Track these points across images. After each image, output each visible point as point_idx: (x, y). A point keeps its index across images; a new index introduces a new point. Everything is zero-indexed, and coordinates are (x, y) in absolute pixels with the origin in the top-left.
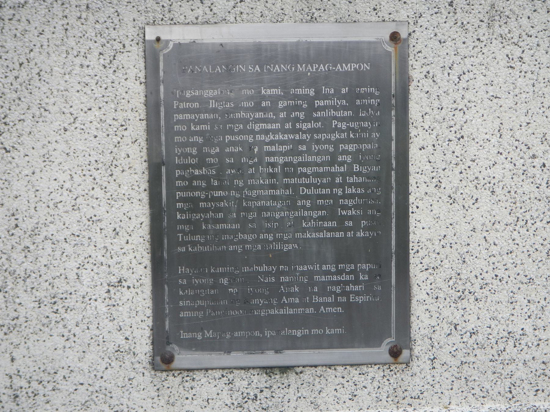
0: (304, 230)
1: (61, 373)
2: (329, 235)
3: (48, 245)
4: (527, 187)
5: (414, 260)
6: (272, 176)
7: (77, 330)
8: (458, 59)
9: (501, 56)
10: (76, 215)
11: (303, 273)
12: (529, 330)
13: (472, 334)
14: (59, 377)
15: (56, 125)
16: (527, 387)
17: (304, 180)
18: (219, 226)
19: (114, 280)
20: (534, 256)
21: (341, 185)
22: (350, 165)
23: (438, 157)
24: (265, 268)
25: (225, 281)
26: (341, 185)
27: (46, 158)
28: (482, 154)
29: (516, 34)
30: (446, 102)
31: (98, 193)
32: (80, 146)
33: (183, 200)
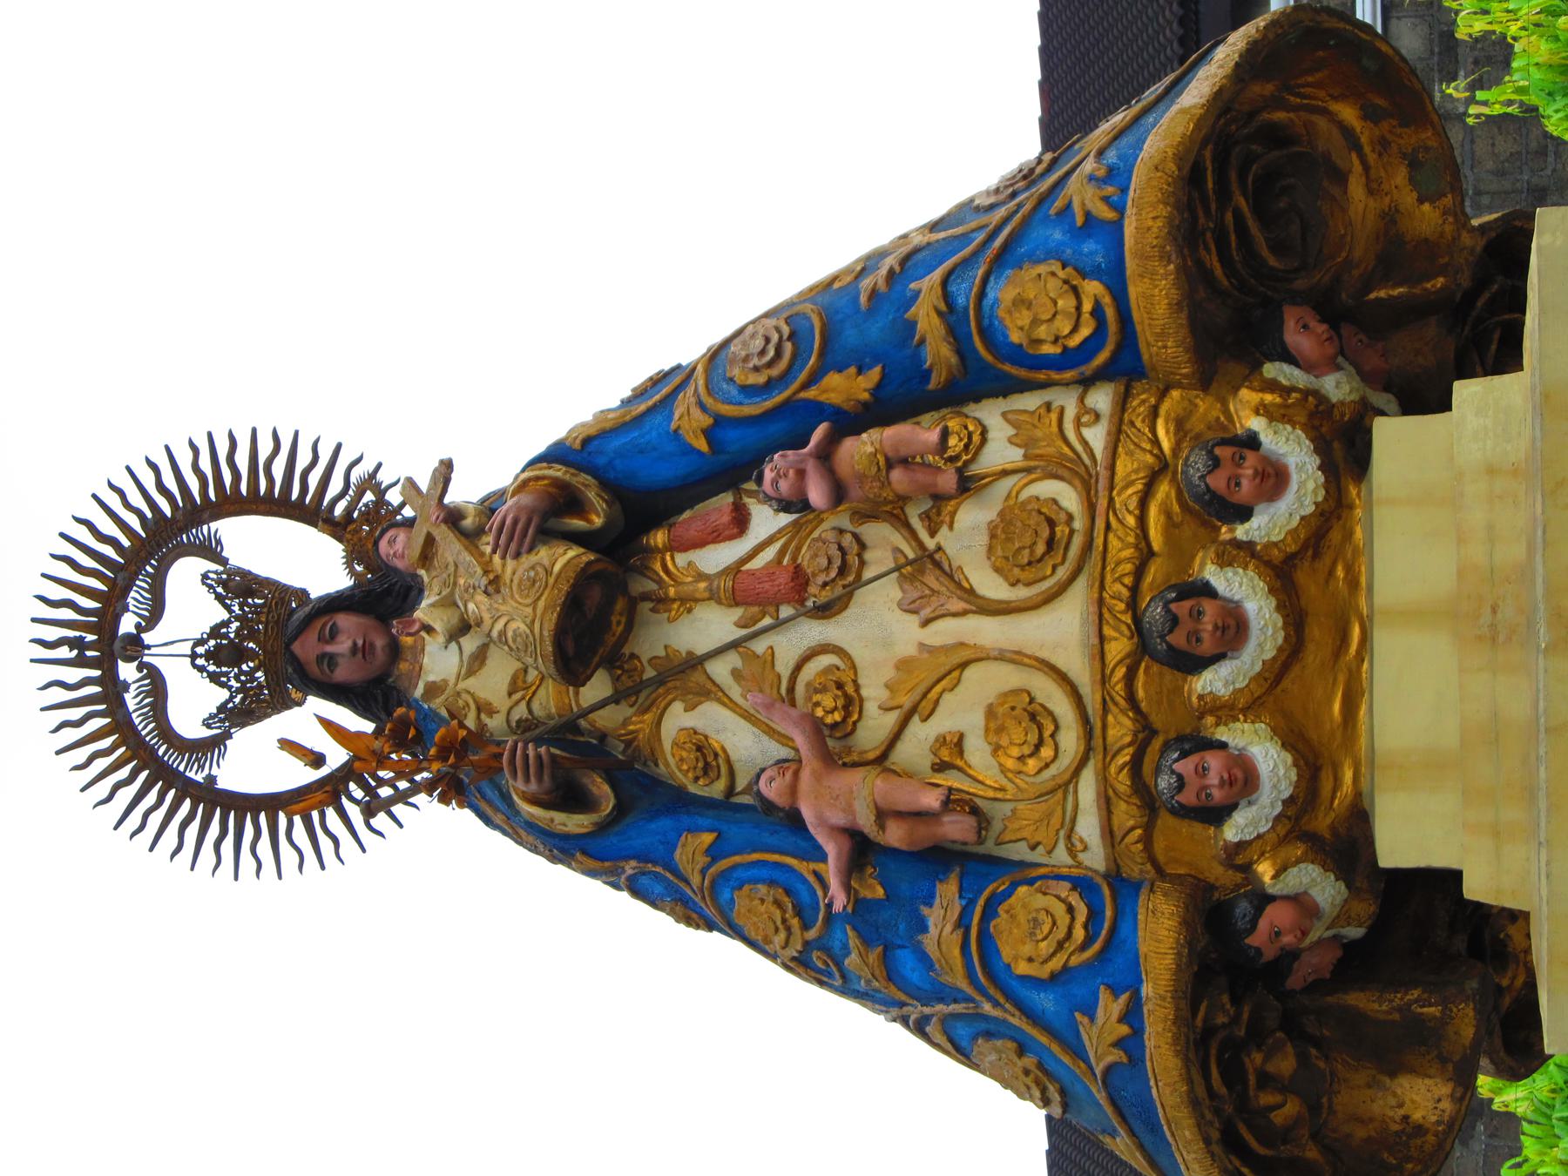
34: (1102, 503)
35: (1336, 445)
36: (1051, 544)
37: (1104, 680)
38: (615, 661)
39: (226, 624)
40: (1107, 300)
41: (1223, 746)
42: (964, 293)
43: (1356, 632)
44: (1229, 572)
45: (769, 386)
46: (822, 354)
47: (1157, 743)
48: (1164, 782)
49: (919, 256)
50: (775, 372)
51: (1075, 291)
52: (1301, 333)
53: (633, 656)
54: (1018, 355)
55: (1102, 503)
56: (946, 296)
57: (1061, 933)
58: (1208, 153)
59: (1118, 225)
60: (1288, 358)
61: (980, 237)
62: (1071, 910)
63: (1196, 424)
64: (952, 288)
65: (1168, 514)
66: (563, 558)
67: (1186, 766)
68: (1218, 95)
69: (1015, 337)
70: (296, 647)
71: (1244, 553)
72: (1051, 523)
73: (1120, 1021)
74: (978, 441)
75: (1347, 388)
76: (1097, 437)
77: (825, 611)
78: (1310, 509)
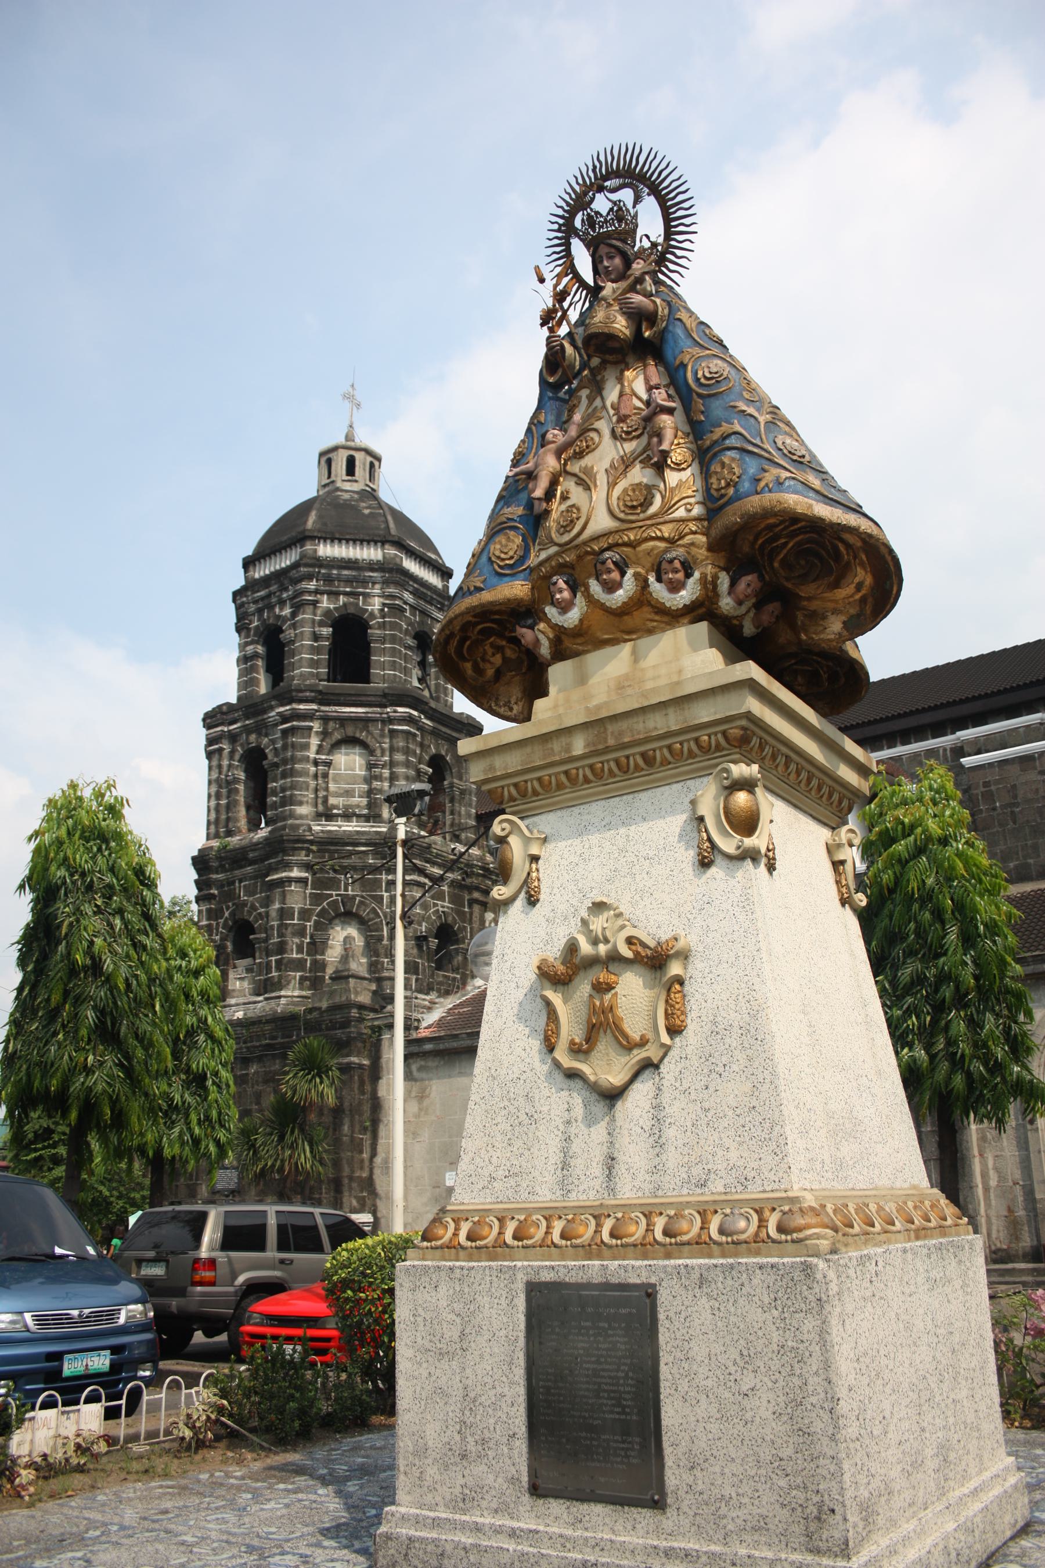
0: (604, 1412)
1: (486, 1488)
2: (617, 1417)
3: (481, 1408)
4: (727, 1395)
5: (664, 1438)
6: (587, 1376)
7: (494, 1462)
8: (683, 1308)
9: (707, 1306)
10: (494, 1391)
11: (604, 1440)
12: (734, 1495)
13: (701, 1493)
14: (484, 1491)
15: (485, 1338)
16: (735, 1537)
17: (604, 1380)
18: (562, 1405)
19: (511, 1433)
20: (734, 1442)
21: (622, 1385)
22: (627, 1374)
23: (675, 1371)
24: (584, 1434)
25: (564, 1440)
26: (622, 1385)
27: (481, 1356)
28: (701, 1370)
29: (715, 1292)
30: (678, 1335)
31: (504, 1379)
32: (496, 1350)
33: (543, 1387)
34: (649, 522)
35: (704, 610)
36: (634, 507)
37: (585, 543)
38: (604, 363)
39: (601, 216)
40: (726, 499)
41: (575, 596)
42: (732, 441)
43: (634, 637)
44: (633, 579)
45: (698, 380)
46: (710, 396)
47: (570, 571)
48: (555, 578)
49: (752, 420)
50: (703, 381)
51: (728, 485)
52: (748, 583)
53: (605, 369)
54: (708, 470)
55: (649, 522)
56: (729, 435)
57: (503, 556)
58: (803, 523)
59: (758, 493)
60: (733, 584)
61: (757, 441)
62: (512, 558)
63: (694, 550)
64: (733, 437)
65: (652, 550)
66: (621, 325)
67: (561, 584)
68: (821, 520)
69: (712, 468)
70: (602, 246)
71: (643, 584)
72: (641, 505)
73: (475, 587)
74: (678, 467)
75: (728, 608)
76: (681, 513)
77: (614, 434)
78: (668, 605)
